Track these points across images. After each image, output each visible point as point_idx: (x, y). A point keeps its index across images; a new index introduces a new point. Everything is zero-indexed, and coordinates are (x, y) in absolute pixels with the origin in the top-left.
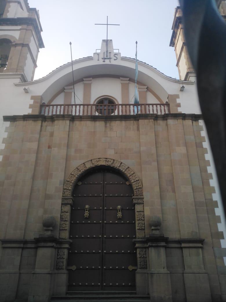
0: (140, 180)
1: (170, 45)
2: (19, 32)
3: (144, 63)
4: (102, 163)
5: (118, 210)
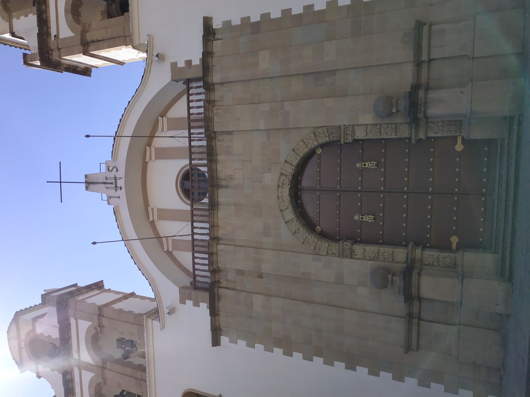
0: (314, 132)
1: (90, 75)
3: (120, 121)
4: (286, 192)
5: (363, 167)
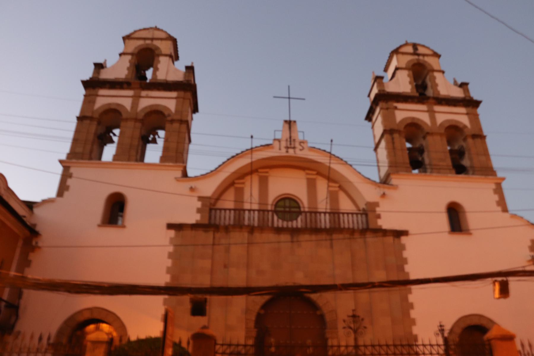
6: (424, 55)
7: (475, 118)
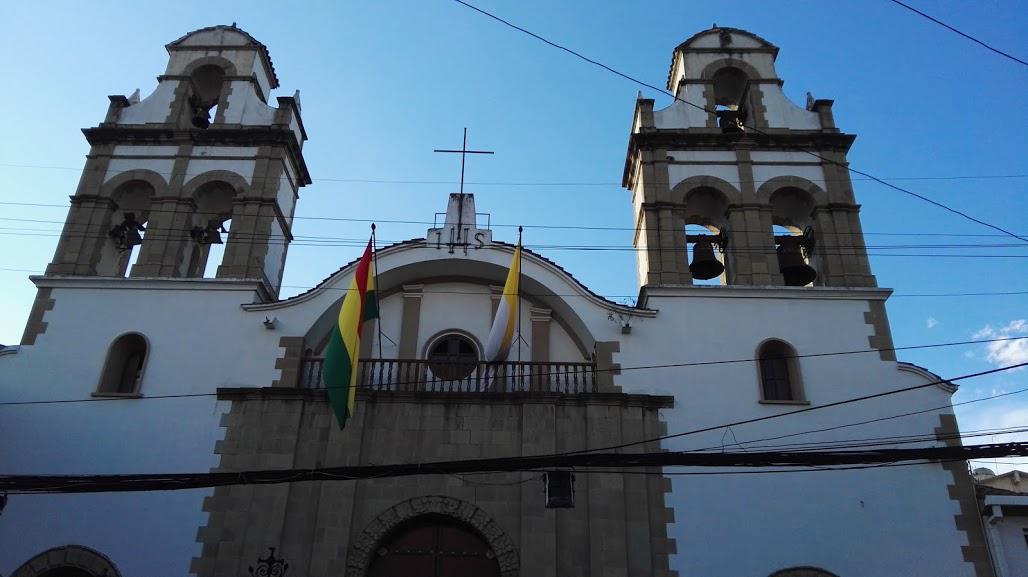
1: (624, 186)
2: (252, 163)
6: (742, 51)
7: (838, 172)
